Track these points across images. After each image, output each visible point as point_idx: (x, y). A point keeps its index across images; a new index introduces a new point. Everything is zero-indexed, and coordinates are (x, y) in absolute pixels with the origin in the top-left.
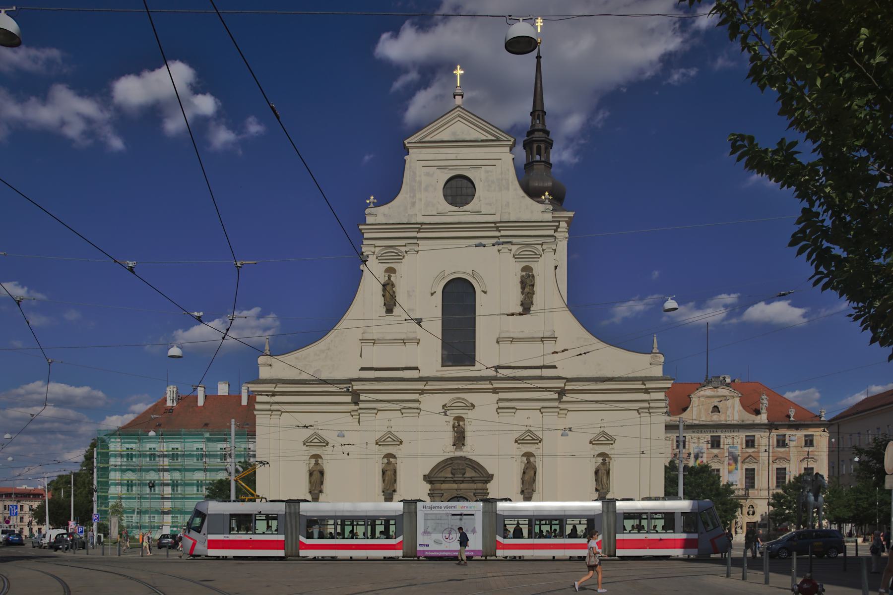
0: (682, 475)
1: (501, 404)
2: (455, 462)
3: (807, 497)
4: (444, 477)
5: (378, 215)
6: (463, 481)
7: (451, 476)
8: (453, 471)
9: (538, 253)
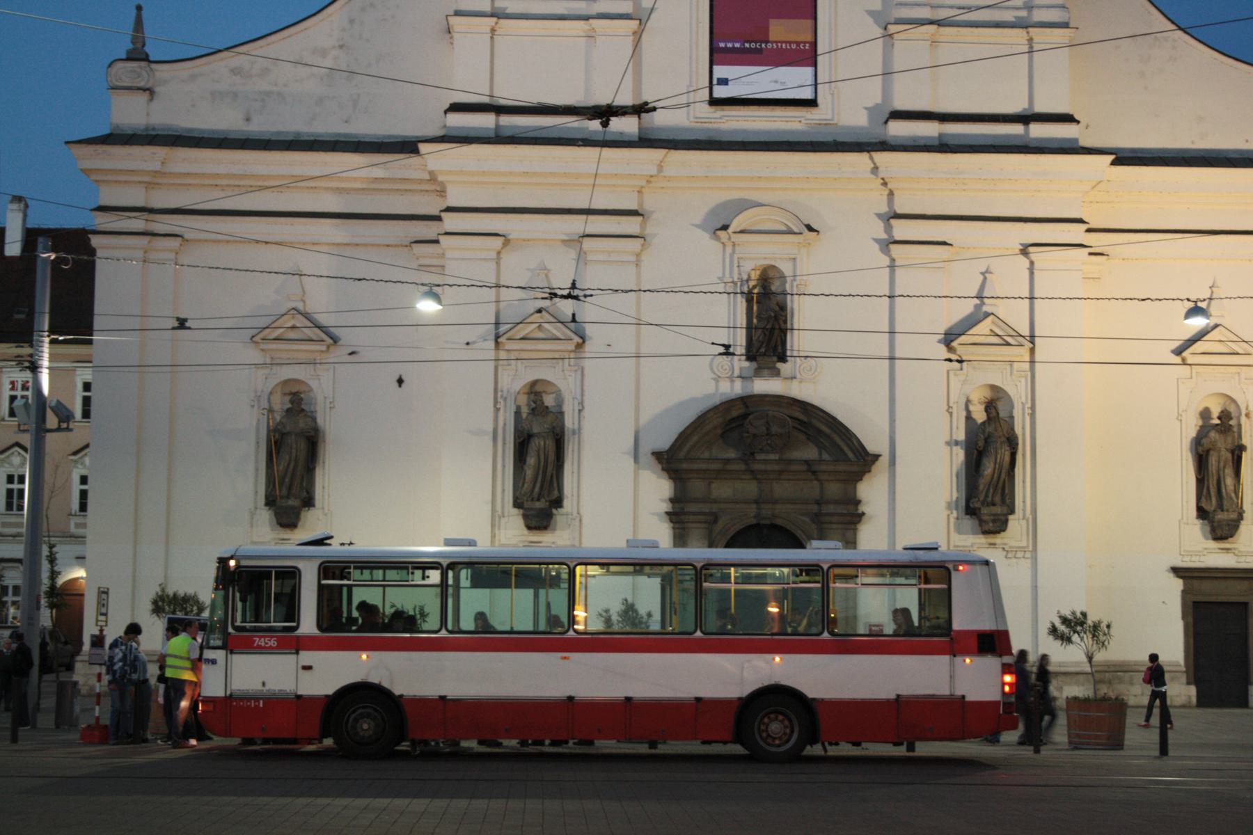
1: (902, 230)
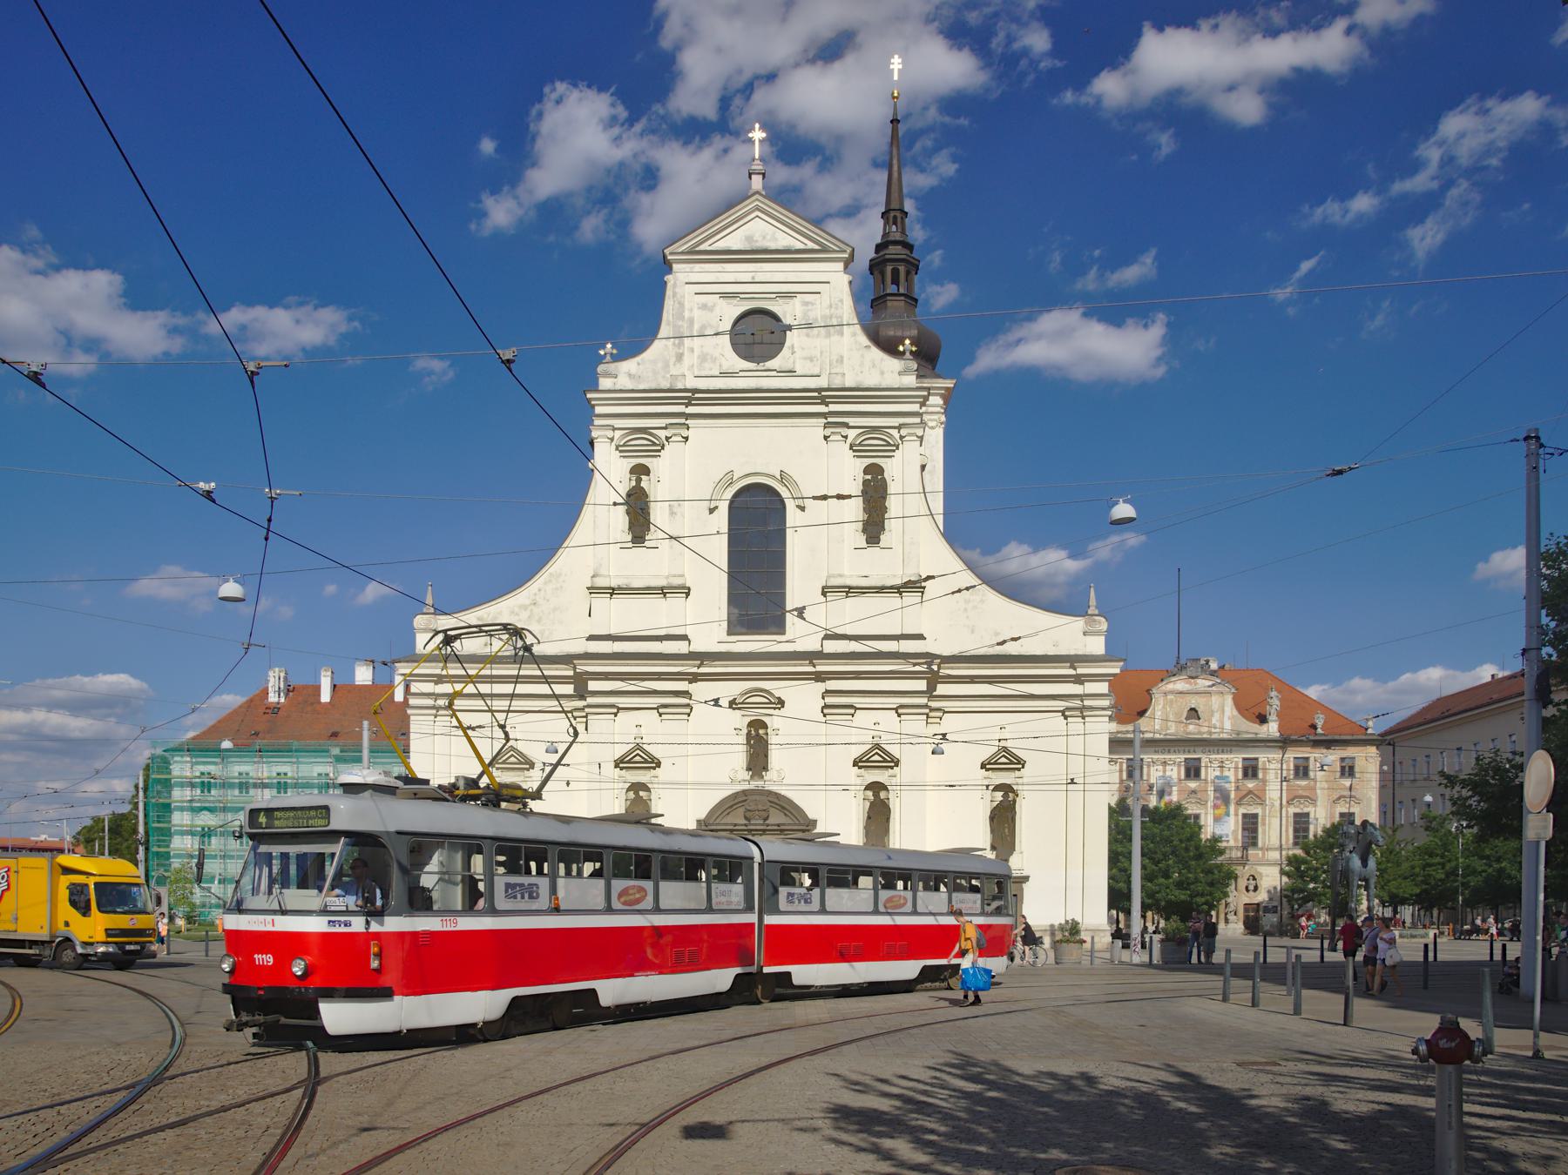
0: (1139, 823)
1: (830, 700)
2: (754, 797)
3: (1348, 860)
4: (731, 824)
5: (622, 375)
6: (764, 831)
7: (746, 822)
8: (748, 814)
9: (892, 443)
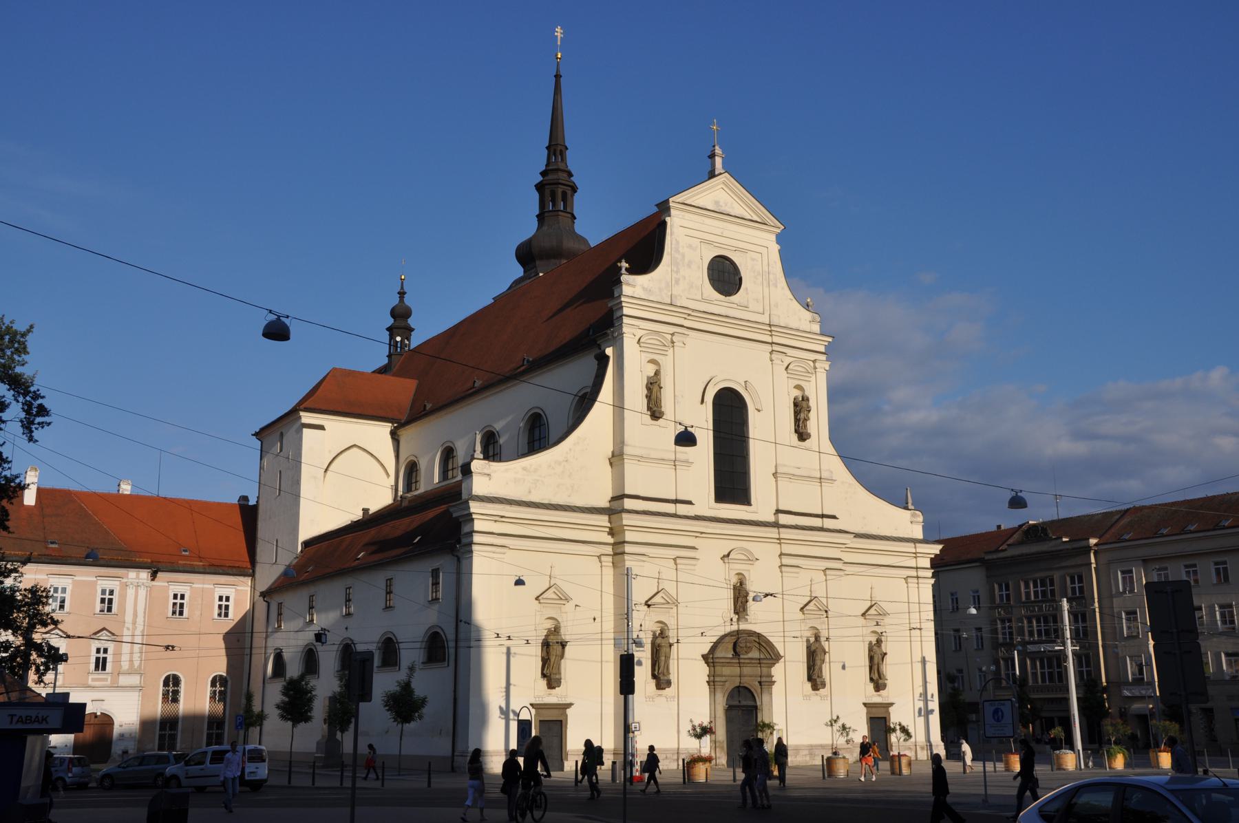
1: (786, 561)
